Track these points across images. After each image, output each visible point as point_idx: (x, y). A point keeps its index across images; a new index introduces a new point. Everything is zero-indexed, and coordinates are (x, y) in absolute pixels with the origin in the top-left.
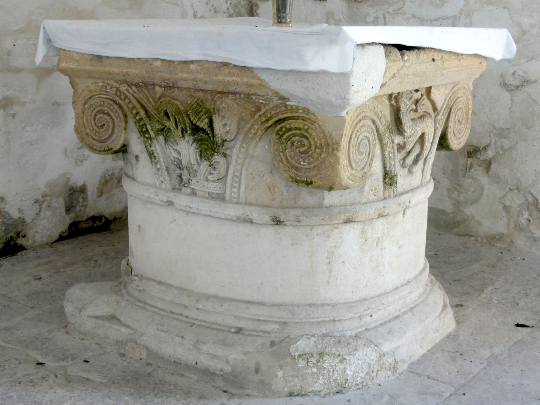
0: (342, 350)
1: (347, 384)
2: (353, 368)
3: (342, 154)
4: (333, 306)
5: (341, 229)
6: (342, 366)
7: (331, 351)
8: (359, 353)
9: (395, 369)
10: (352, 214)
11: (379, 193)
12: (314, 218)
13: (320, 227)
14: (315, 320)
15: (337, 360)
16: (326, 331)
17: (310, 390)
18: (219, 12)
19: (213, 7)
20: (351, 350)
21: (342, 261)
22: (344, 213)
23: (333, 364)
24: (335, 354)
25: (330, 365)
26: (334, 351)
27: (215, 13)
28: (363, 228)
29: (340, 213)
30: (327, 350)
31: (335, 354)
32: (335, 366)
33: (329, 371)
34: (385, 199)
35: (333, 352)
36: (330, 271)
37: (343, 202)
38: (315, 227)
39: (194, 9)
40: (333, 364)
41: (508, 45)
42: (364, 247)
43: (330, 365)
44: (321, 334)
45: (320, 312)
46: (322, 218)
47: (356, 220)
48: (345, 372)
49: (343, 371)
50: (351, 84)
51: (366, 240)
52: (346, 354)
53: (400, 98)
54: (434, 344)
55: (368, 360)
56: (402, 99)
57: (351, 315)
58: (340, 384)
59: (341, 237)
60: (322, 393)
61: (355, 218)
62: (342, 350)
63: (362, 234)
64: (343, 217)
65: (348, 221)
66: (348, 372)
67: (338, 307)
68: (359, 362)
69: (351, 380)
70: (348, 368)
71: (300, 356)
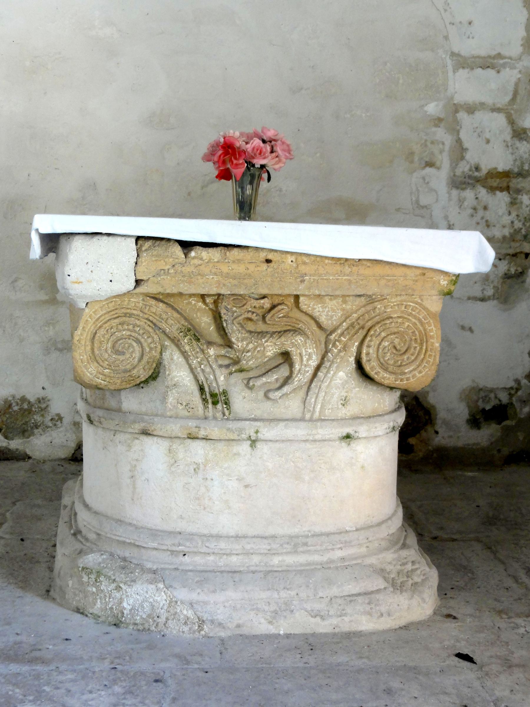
0: (119, 576)
1: (124, 619)
2: (131, 601)
3: (79, 347)
4: (136, 528)
5: (142, 441)
6: (118, 595)
7: (108, 573)
8: (138, 586)
9: (200, 628)
10: (148, 426)
11: (195, 409)
12: (111, 421)
13: (122, 434)
14: (118, 538)
15: (113, 586)
16: (130, 555)
17: (91, 611)
18: (494, 226)
19: (484, 220)
20: (128, 579)
21: (146, 479)
22: (139, 422)
23: (109, 589)
24: (110, 577)
25: (107, 589)
26: (111, 573)
27: (486, 228)
28: (171, 446)
29: (134, 422)
30: (104, 571)
31: (110, 577)
32: (111, 591)
33: (105, 596)
34: (206, 418)
35: (109, 574)
36: (134, 488)
37: (144, 409)
38: (117, 432)
39: (448, 221)
40: (109, 589)
41: (481, 253)
42: (173, 469)
43: (107, 589)
44: (123, 556)
45: (121, 530)
46: (117, 423)
47: (155, 433)
48: (121, 603)
49: (120, 600)
50: (66, 273)
51: (176, 462)
52: (121, 582)
53: (219, 303)
54: (312, 632)
55: (151, 600)
56: (222, 304)
57: (155, 545)
58: (116, 615)
59: (142, 450)
60: (101, 620)
61: (153, 431)
62: (119, 576)
63: (170, 453)
64: (138, 427)
65: (145, 433)
66: (125, 605)
67: (141, 530)
68: (138, 597)
69: (129, 616)
70: (125, 599)
71: (83, 568)
